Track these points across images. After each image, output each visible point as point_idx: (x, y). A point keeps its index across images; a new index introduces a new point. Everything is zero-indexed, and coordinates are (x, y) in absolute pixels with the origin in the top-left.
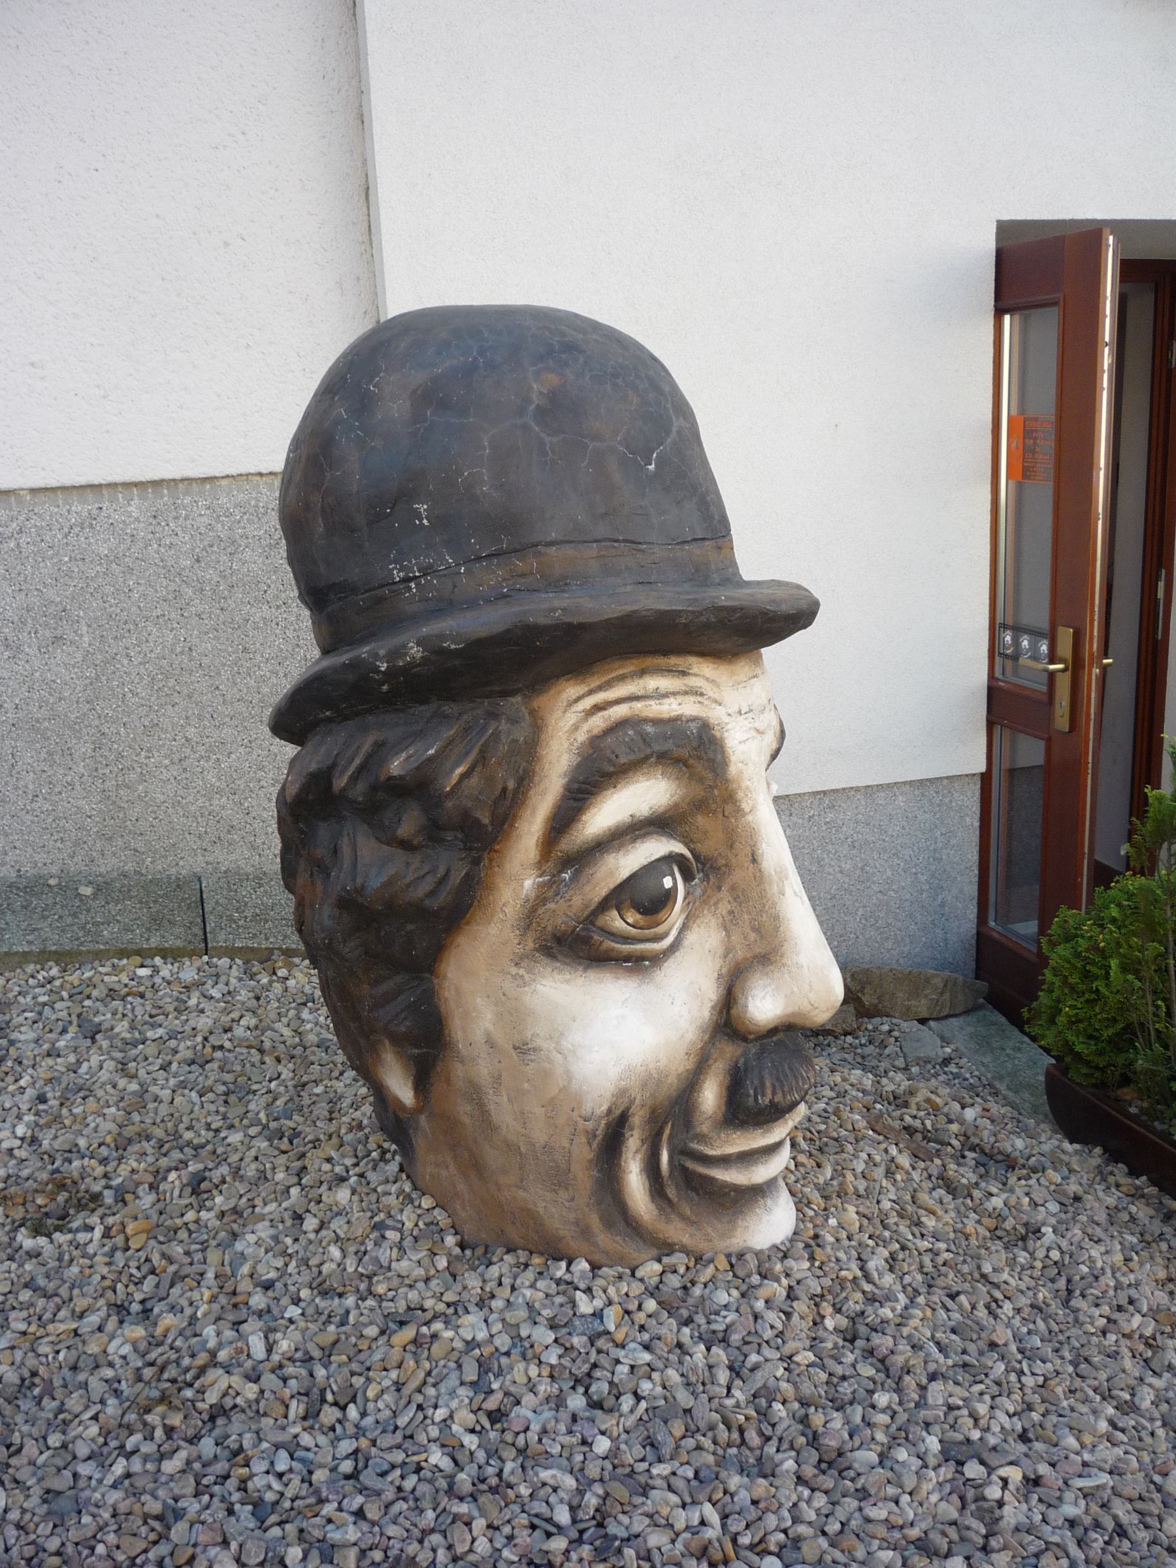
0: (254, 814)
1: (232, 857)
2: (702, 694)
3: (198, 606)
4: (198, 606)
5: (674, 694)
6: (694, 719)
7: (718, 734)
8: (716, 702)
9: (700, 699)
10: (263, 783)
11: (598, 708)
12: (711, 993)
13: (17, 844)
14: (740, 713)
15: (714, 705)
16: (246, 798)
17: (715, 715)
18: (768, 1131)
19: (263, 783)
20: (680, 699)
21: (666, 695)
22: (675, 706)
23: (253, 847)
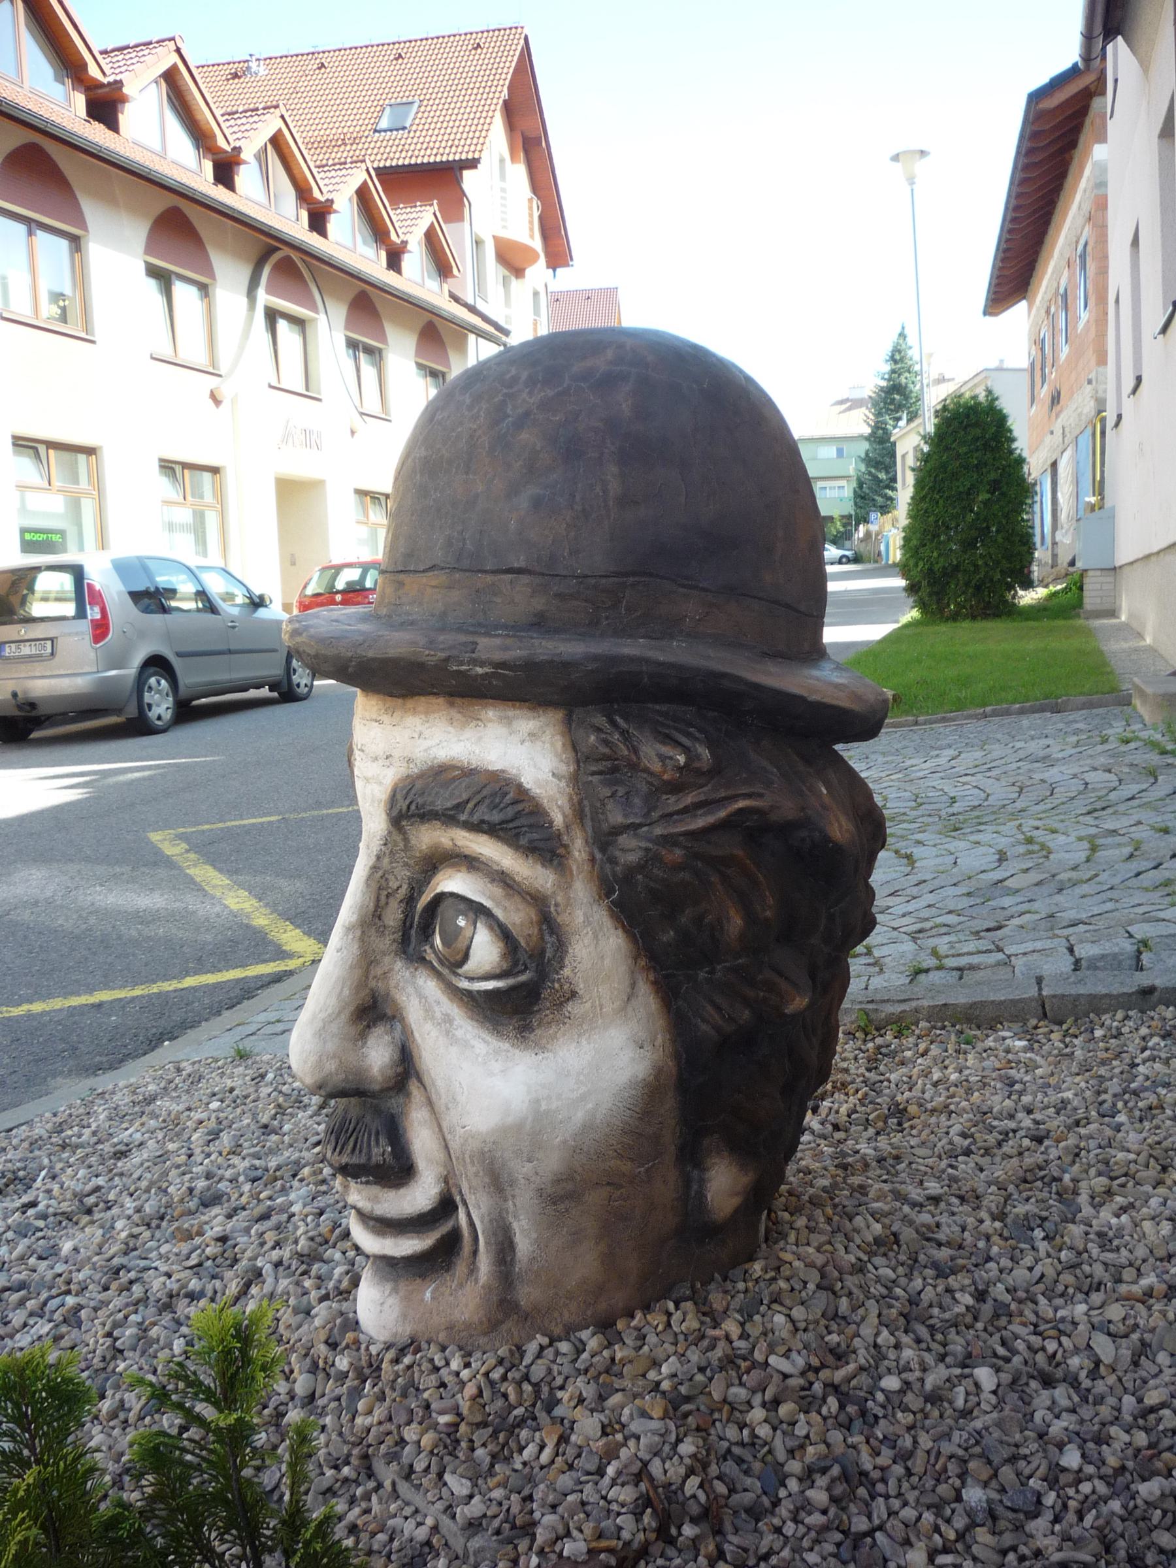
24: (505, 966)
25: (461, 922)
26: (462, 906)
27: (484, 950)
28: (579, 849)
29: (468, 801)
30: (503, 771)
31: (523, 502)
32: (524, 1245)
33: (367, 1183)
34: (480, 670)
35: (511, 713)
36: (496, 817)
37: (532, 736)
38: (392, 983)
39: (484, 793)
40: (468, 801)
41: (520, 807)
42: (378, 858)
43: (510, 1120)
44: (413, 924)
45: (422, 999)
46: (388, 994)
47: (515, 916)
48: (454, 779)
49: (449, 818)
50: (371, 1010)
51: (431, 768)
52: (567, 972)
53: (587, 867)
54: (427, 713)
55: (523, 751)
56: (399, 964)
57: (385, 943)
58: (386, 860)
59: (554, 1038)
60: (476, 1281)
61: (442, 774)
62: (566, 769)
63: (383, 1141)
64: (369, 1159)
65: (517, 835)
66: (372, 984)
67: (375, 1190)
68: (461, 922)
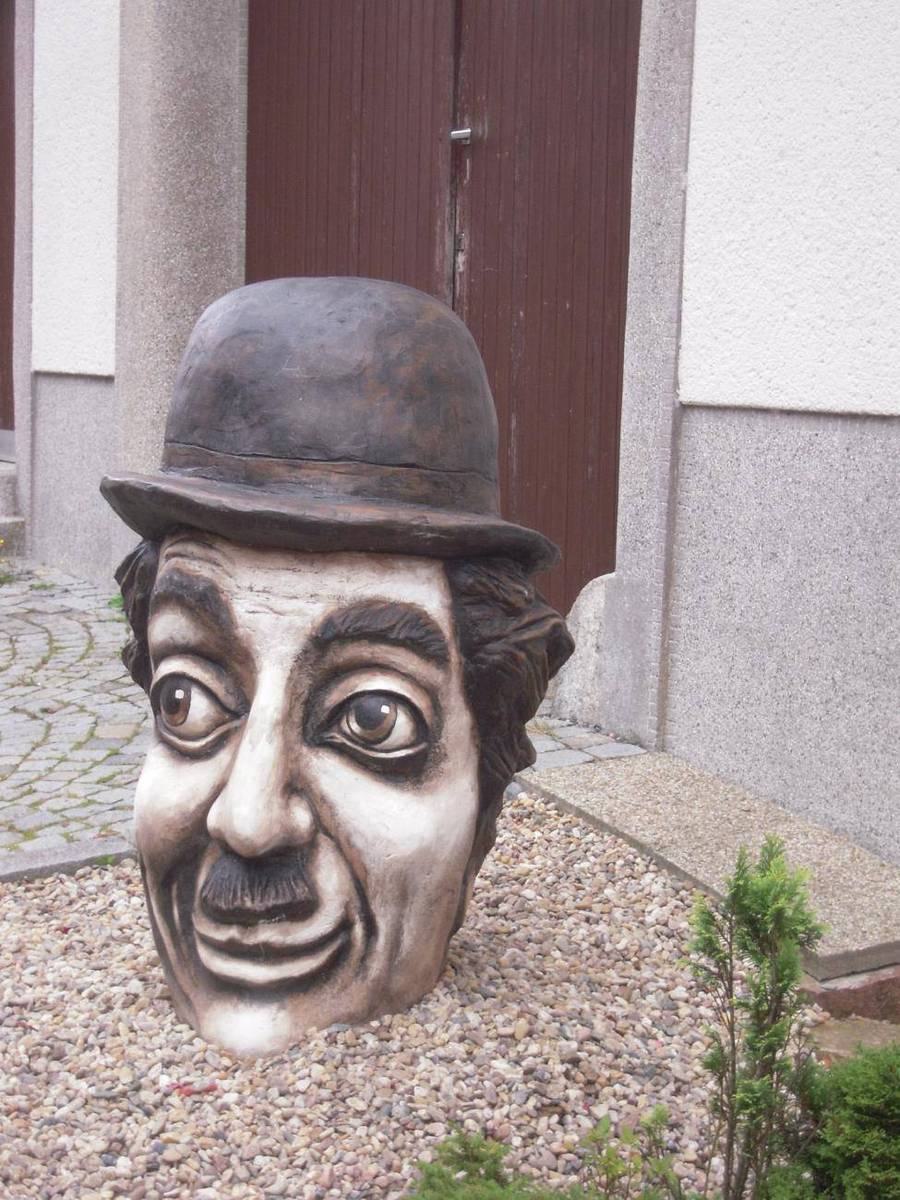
0: (864, 778)
1: (844, 817)
2: (218, 565)
3: (862, 547)
4: (862, 547)
5: (200, 559)
6: (206, 580)
7: (224, 598)
8: (228, 573)
9: (214, 568)
10: (875, 747)
11: (169, 557)
12: (204, 793)
13: (722, 744)
14: (251, 589)
15: (225, 576)
16: (862, 759)
17: (226, 583)
18: (218, 928)
19: (875, 747)
20: (201, 563)
21: (195, 558)
22: (197, 568)
23: (858, 814)
24: (413, 739)
25: (385, 709)
26: (382, 699)
27: (403, 727)
28: (454, 656)
29: (397, 623)
30: (413, 604)
31: (408, 418)
32: (407, 940)
33: (280, 921)
34: (429, 535)
35: (414, 564)
36: (415, 634)
37: (429, 580)
38: (302, 764)
39: (407, 618)
40: (397, 623)
41: (428, 627)
42: (291, 671)
43: (425, 844)
44: (315, 722)
45: (331, 774)
46: (299, 774)
47: (420, 701)
48: (381, 610)
49: (380, 637)
50: (294, 786)
51: (360, 602)
52: (443, 740)
53: (457, 667)
54: (351, 564)
55: (421, 591)
56: (305, 750)
57: (295, 734)
58: (296, 673)
59: (436, 787)
60: (364, 978)
61: (370, 607)
62: (448, 601)
63: (301, 884)
64: (294, 897)
65: (425, 648)
66: (290, 766)
67: (286, 925)
68: (385, 709)
